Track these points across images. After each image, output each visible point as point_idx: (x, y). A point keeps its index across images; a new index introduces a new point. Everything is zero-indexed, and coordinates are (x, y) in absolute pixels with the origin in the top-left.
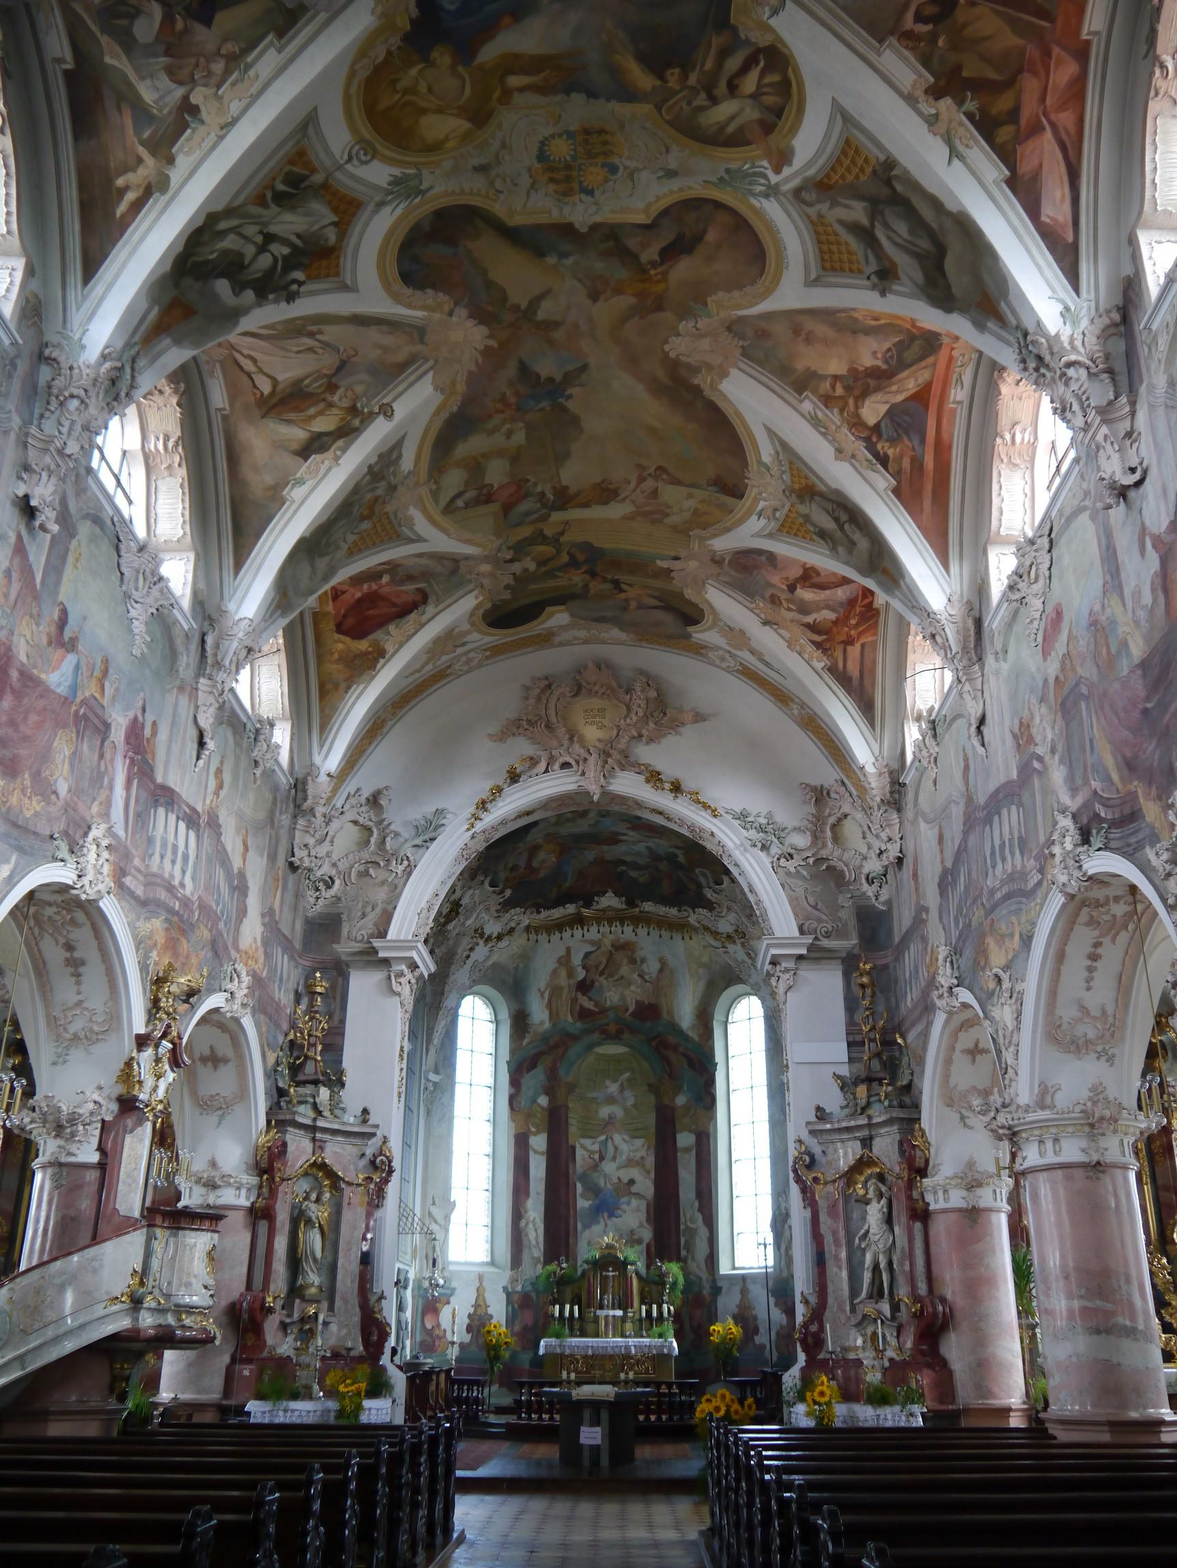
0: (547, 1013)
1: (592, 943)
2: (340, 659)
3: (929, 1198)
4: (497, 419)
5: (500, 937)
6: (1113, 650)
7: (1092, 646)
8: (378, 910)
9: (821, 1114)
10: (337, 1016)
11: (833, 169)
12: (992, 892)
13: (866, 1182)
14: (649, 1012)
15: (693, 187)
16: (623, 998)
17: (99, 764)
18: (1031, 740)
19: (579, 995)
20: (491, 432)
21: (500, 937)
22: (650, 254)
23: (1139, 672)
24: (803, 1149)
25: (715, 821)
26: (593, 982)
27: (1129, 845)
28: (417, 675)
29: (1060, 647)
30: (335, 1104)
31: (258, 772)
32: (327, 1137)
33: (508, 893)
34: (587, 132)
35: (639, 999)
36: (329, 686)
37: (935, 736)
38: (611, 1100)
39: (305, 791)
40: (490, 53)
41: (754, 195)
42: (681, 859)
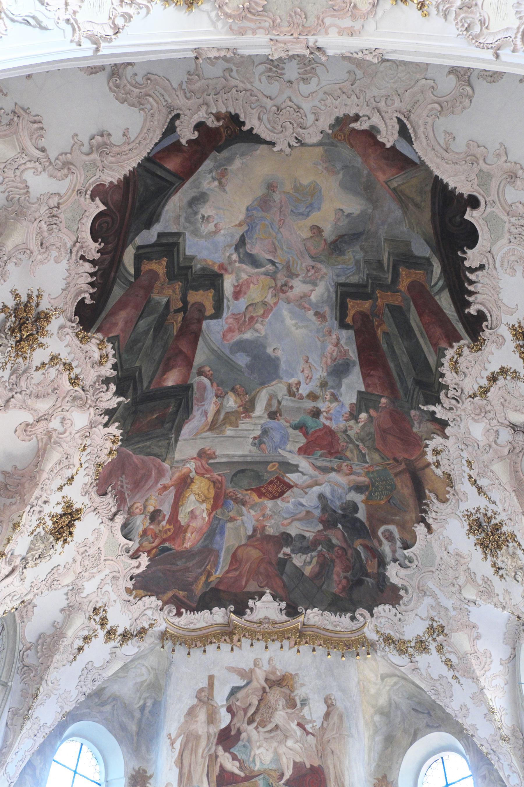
0: (176, 771)
1: (242, 673)
5: (126, 636)
16: (277, 759)
21: (126, 636)
26: (239, 732)
35: (298, 759)
42: (361, 515)
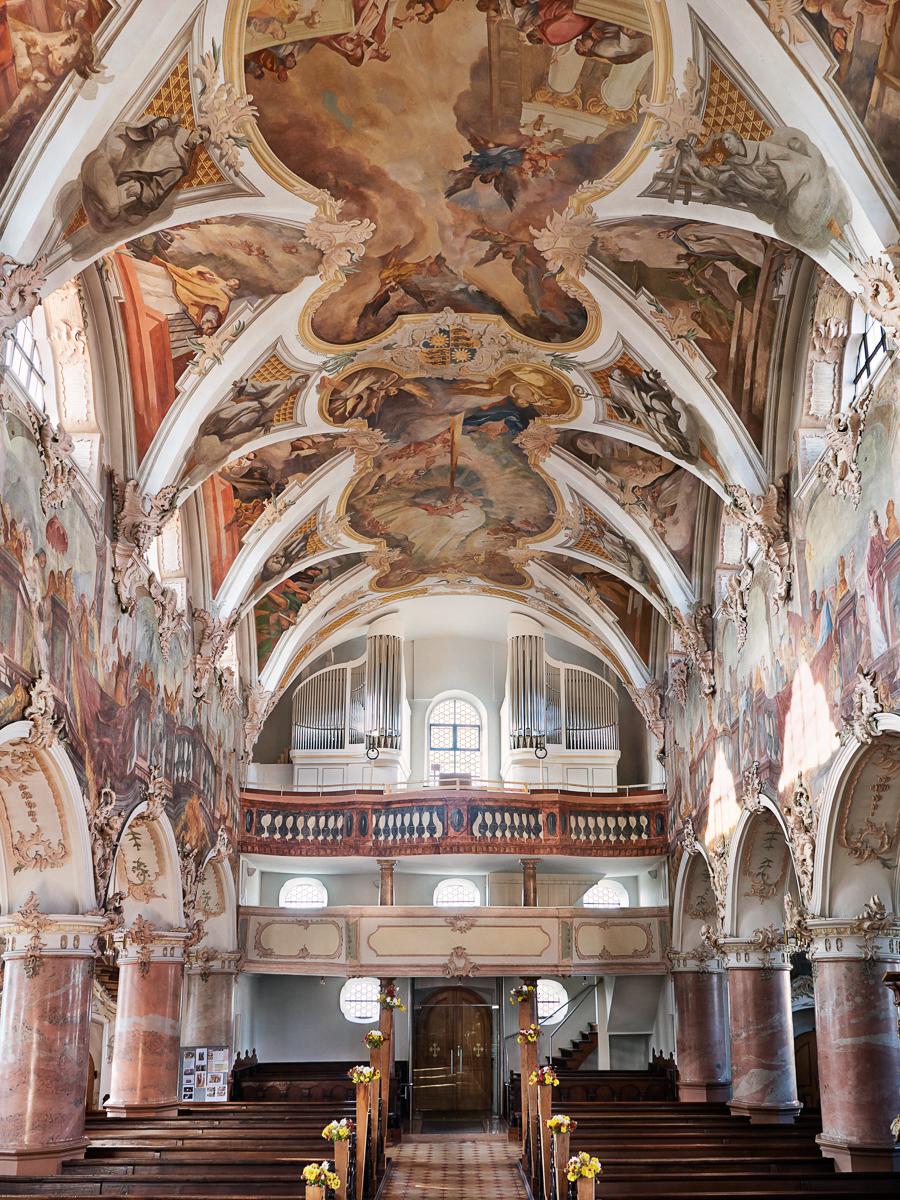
4: (548, 147)
11: (293, 403)
15: (370, 344)
20: (557, 133)
22: (394, 297)
34: (444, 363)
40: (497, 398)
41: (335, 358)
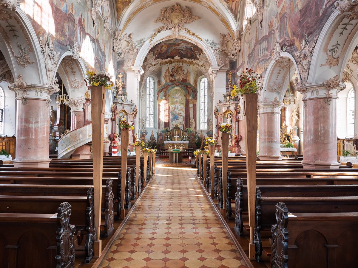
1: (173, 66)
2: (121, 3)
3: (239, 118)
5: (155, 65)
6: (294, 6)
7: (289, 5)
8: (132, 60)
9: (220, 102)
10: (125, 82)
12: (259, 59)
13: (228, 114)
14: (184, 81)
16: (179, 78)
17: (74, 29)
18: (272, 26)
19: (171, 77)
21: (155, 65)
23: (300, 12)
24: (216, 108)
25: (201, 42)
27: (291, 51)
28: (138, 7)
29: (282, 5)
30: (126, 100)
31: (105, 30)
32: (124, 105)
33: (156, 56)
36: (119, 9)
37: (250, 24)
38: (177, 98)
39: (115, 34)
42: (192, 49)
